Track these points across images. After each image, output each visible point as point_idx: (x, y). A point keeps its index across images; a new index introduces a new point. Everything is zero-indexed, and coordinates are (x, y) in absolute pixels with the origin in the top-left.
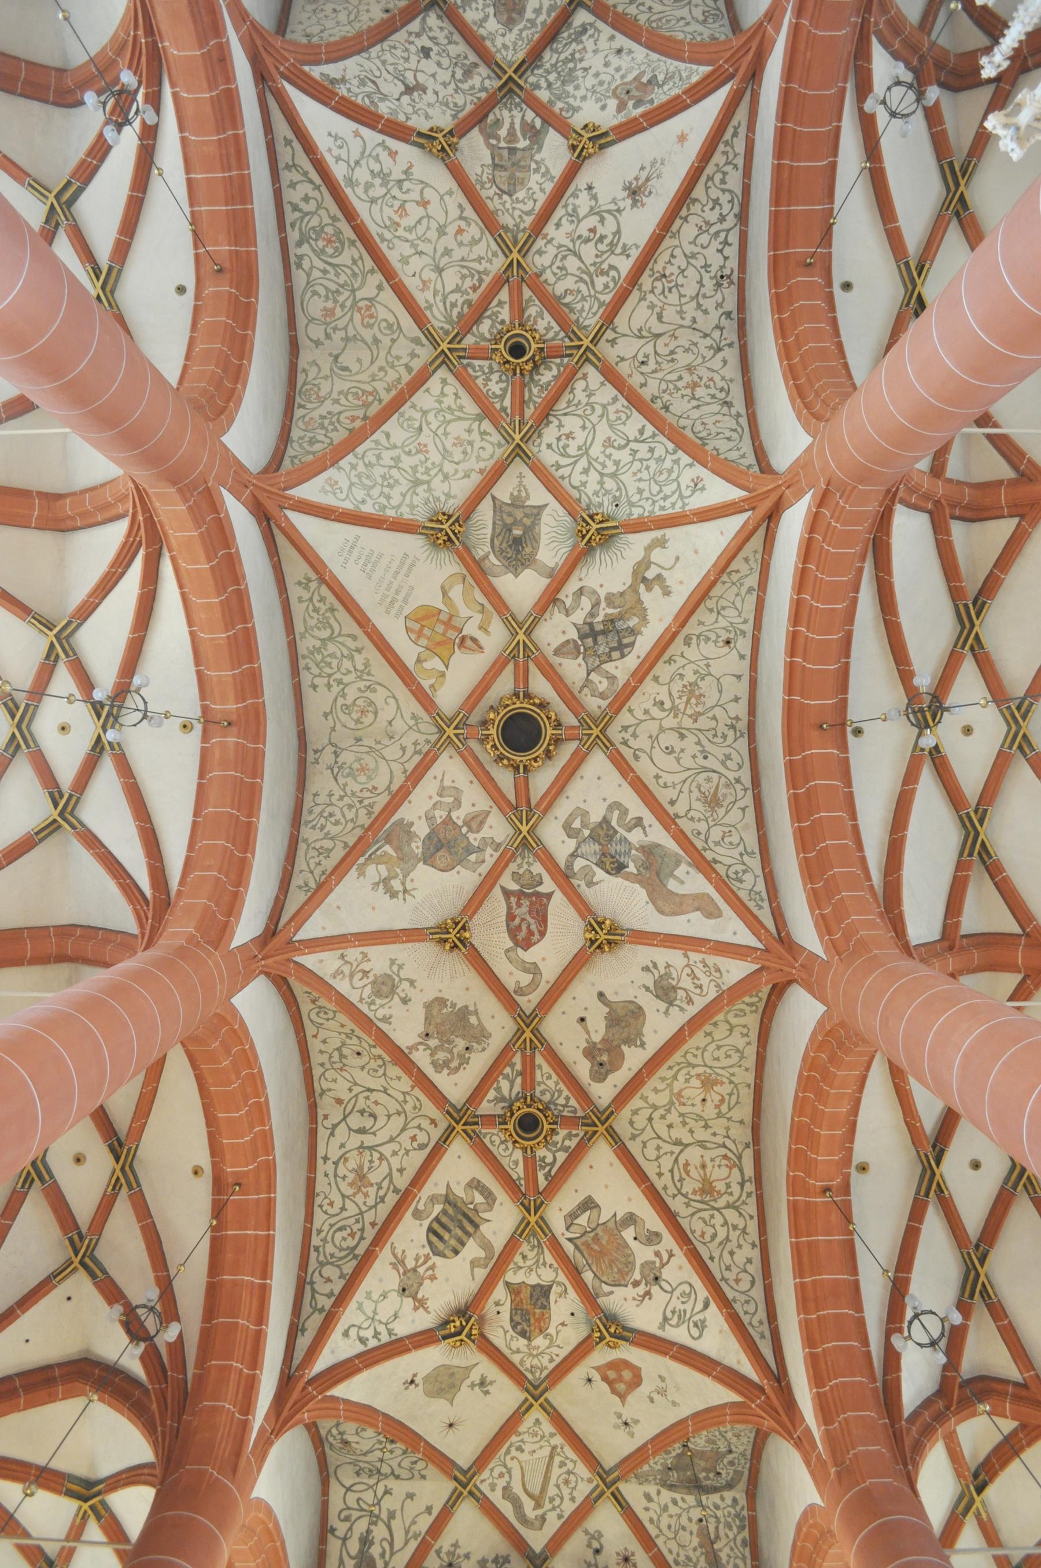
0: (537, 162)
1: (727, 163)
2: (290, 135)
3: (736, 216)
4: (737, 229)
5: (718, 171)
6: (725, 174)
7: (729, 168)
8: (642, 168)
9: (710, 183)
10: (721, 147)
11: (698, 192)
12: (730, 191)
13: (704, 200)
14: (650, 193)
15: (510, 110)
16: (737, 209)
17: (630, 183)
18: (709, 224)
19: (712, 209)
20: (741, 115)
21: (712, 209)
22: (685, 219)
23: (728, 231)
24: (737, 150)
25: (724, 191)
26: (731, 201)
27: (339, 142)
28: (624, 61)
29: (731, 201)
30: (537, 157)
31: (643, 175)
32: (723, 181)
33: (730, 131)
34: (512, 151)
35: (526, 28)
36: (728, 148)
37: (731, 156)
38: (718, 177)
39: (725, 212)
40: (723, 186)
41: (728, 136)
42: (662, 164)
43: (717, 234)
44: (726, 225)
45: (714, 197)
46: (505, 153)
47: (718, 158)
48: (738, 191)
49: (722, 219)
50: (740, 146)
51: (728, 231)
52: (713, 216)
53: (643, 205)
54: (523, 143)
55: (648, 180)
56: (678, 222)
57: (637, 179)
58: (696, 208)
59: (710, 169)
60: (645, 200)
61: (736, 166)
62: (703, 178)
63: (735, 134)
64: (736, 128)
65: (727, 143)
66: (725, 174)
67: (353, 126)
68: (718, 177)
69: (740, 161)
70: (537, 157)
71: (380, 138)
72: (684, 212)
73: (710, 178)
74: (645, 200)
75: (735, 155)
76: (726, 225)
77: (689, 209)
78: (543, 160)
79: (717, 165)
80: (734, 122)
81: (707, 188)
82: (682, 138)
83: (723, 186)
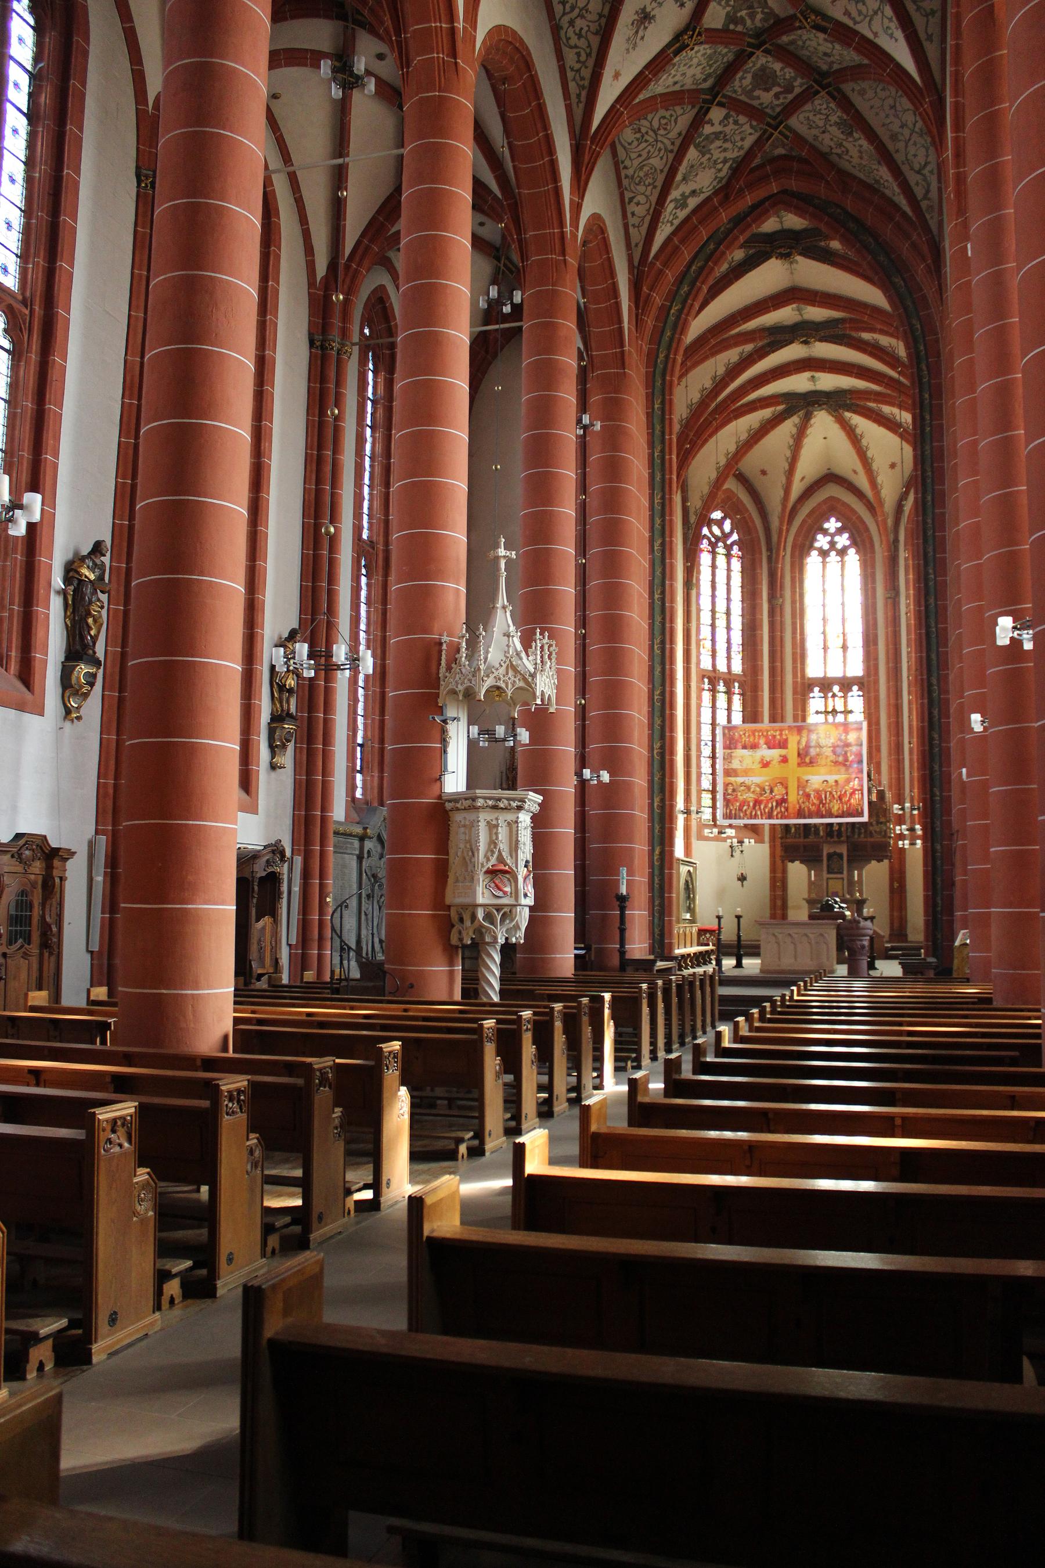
0: (729, 6)
1: (578, 71)
2: (926, 44)
3: (562, 28)
4: (557, 17)
5: (584, 63)
6: (578, 61)
7: (577, 66)
8: (642, 38)
9: (588, 51)
10: (586, 83)
11: (595, 41)
12: (571, 47)
13: (590, 36)
14: (633, 24)
15: (756, 27)
16: (562, 33)
17: (650, 23)
18: (582, 17)
19: (581, 29)
20: (579, 112)
21: (581, 29)
22: (600, 16)
23: (564, 14)
24: (574, 83)
25: (576, 47)
26: (568, 39)
27: (890, 32)
28: (671, 81)
29: (568, 39)
30: (728, 9)
31: (641, 33)
32: (578, 54)
33: (583, 98)
34: (751, 7)
35: (751, 68)
36: (581, 83)
37: (578, 77)
38: (583, 58)
39: (571, 29)
40: (577, 50)
41: (584, 94)
42: (628, 50)
43: (573, 8)
44: (566, 18)
45: (582, 40)
46: (756, 5)
47: (586, 73)
48: (565, 50)
49: (572, 23)
50: (572, 85)
51: (564, 14)
52: (579, 23)
53: (637, 12)
54: (743, 13)
55: (637, 32)
56: (606, 12)
57: (646, 28)
58: (594, 27)
59: (591, 63)
60: (636, 17)
61: (572, 69)
62: (594, 55)
63: (579, 96)
64: (579, 102)
65: (583, 87)
66: (578, 61)
67: (878, 41)
68: (583, 58)
69: (570, 75)
70: (728, 9)
71: (857, 27)
72: (603, 21)
73: (588, 55)
74: (636, 17)
75: (574, 79)
76: (566, 18)
77: (600, 25)
78: (724, 8)
79: (586, 67)
80: (582, 106)
81: (589, 46)
82: (617, 76)
83: (577, 50)
